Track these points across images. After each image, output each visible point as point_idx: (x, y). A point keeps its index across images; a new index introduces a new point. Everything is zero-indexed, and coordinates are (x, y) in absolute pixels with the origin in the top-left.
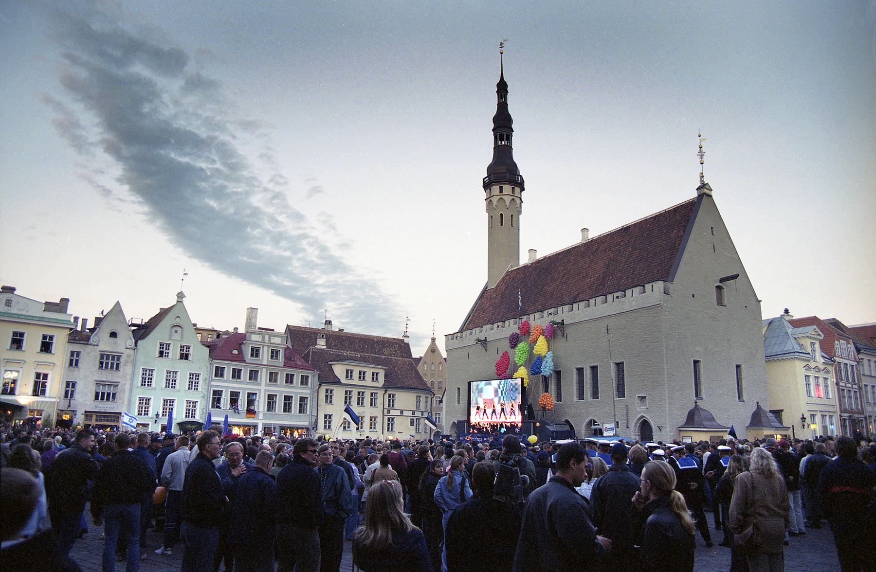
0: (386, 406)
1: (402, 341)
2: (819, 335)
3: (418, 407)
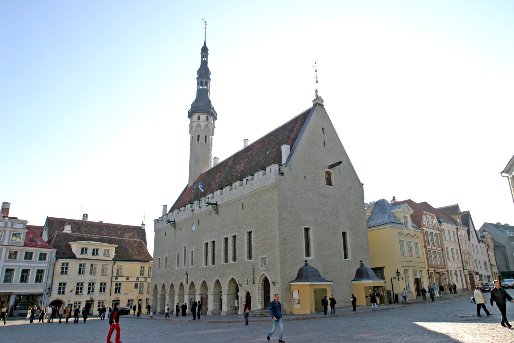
0: (115, 274)
1: (140, 228)
2: (410, 211)
3: (142, 274)
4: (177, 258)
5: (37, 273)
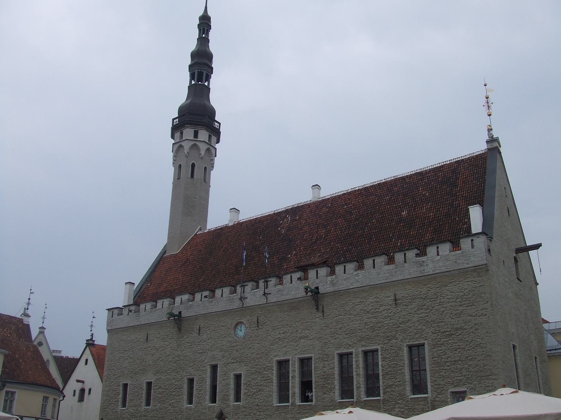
1: (21, 320)
3: (43, 411)
4: (185, 386)
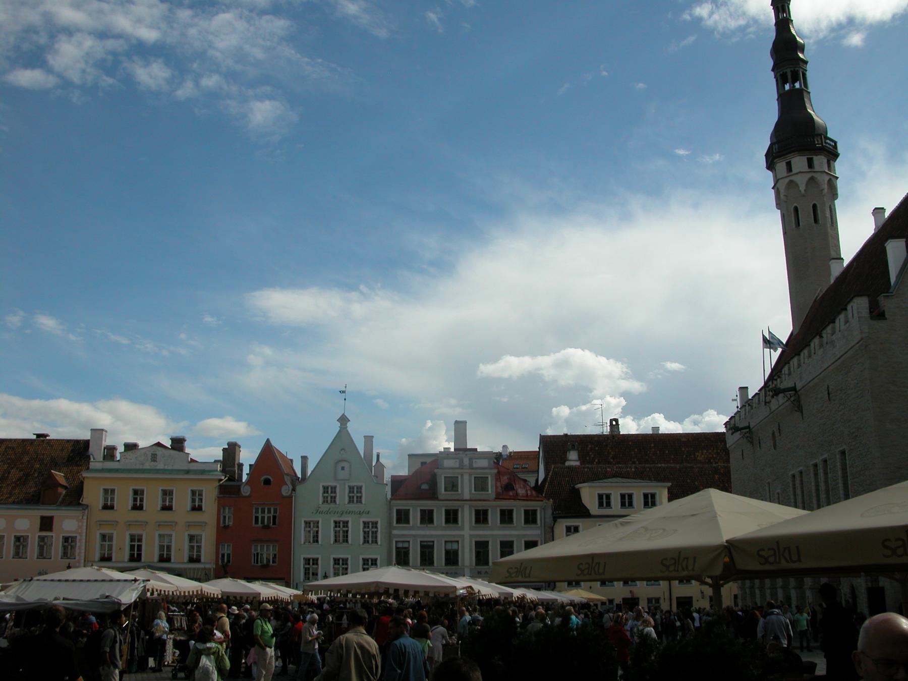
5: (501, 547)
